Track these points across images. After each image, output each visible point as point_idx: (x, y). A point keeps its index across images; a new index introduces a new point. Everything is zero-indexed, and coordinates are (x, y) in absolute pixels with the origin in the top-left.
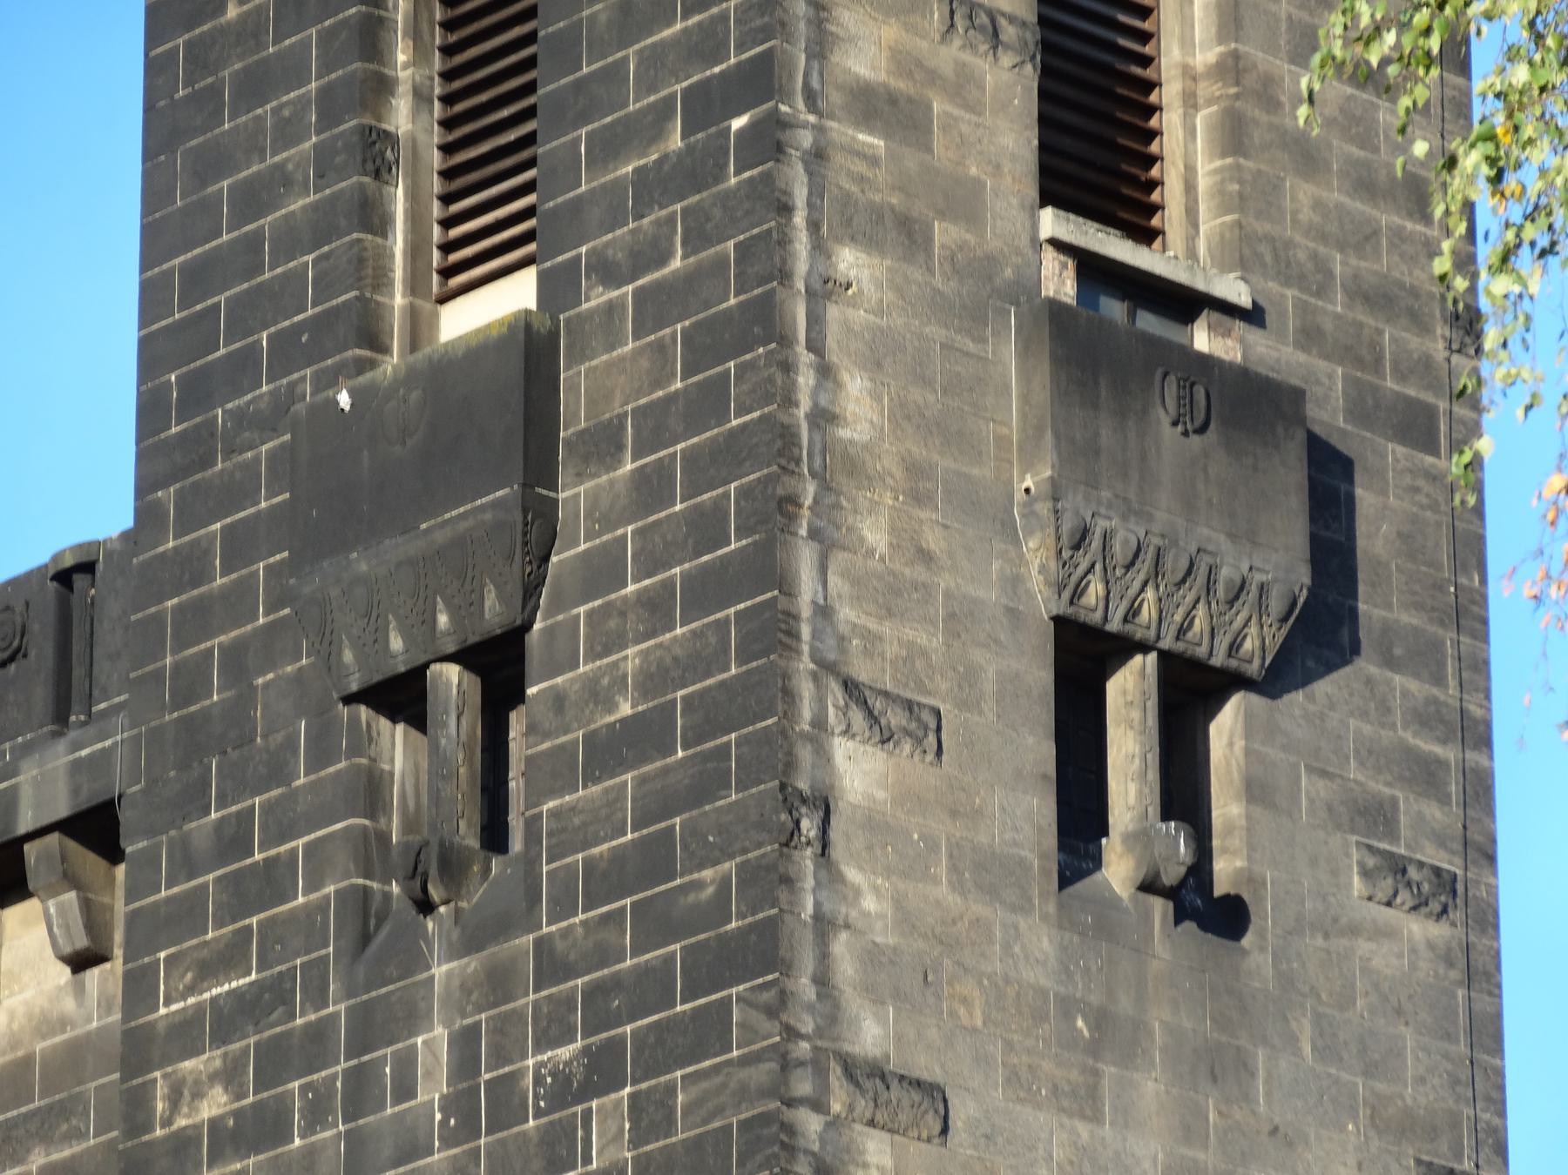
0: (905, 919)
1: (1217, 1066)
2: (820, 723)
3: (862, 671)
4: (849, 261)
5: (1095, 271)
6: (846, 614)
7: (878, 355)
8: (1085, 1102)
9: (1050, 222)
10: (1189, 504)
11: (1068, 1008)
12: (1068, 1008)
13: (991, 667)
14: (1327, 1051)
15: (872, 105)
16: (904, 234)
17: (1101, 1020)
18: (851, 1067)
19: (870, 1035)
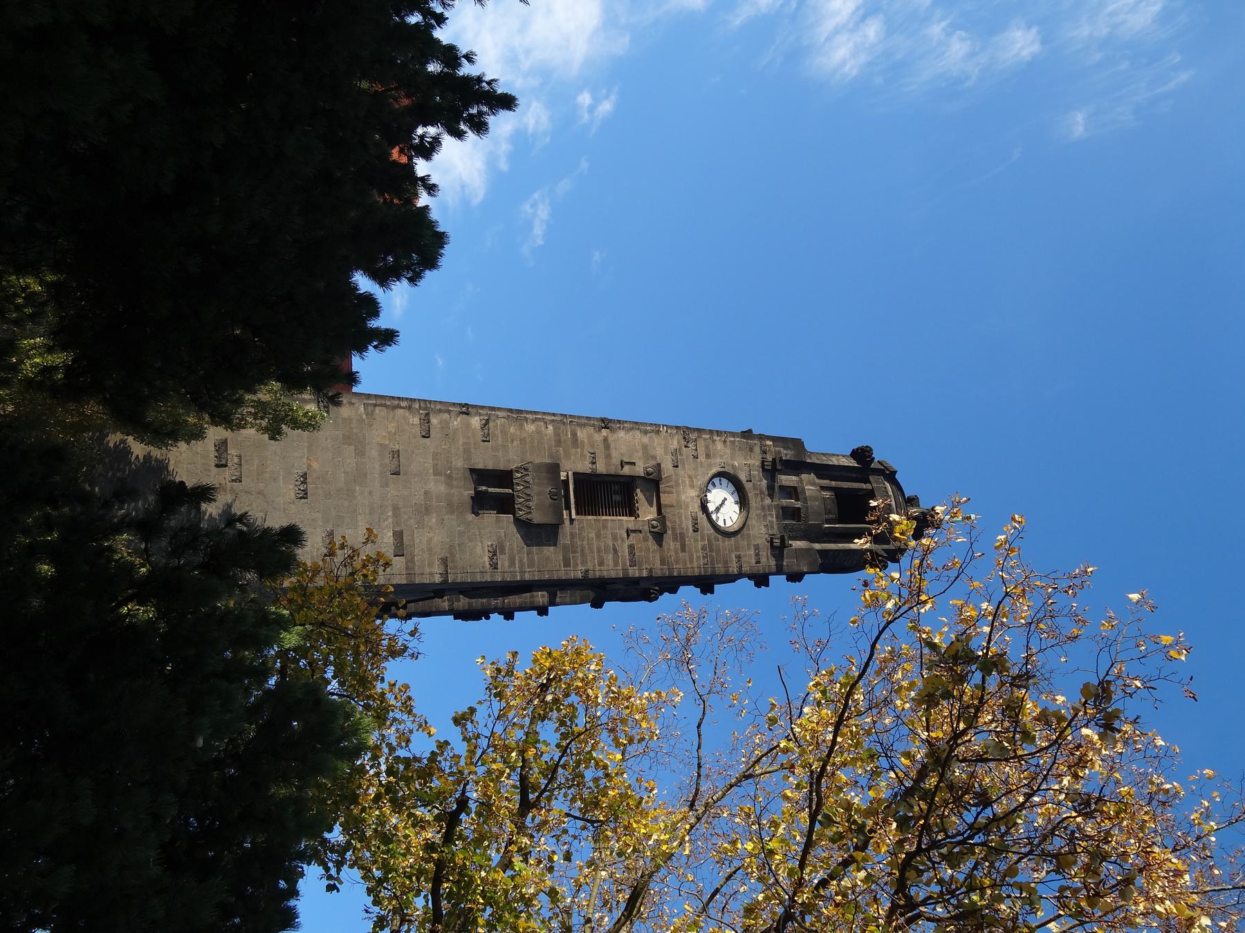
0: (456, 431)
1: (451, 507)
2: (480, 415)
3: (491, 424)
4: (551, 427)
5: (566, 482)
6: (498, 422)
7: (539, 432)
8: (436, 473)
9: (570, 473)
10: (539, 494)
11: (450, 468)
12: (450, 468)
13: (500, 454)
14: (461, 534)
15: (574, 434)
16: (559, 442)
17: (450, 477)
18: (427, 414)
19: (434, 421)
